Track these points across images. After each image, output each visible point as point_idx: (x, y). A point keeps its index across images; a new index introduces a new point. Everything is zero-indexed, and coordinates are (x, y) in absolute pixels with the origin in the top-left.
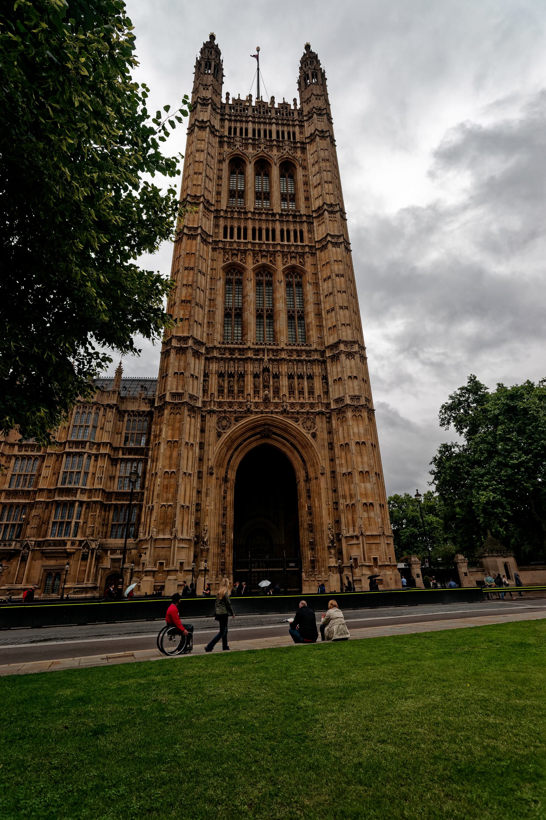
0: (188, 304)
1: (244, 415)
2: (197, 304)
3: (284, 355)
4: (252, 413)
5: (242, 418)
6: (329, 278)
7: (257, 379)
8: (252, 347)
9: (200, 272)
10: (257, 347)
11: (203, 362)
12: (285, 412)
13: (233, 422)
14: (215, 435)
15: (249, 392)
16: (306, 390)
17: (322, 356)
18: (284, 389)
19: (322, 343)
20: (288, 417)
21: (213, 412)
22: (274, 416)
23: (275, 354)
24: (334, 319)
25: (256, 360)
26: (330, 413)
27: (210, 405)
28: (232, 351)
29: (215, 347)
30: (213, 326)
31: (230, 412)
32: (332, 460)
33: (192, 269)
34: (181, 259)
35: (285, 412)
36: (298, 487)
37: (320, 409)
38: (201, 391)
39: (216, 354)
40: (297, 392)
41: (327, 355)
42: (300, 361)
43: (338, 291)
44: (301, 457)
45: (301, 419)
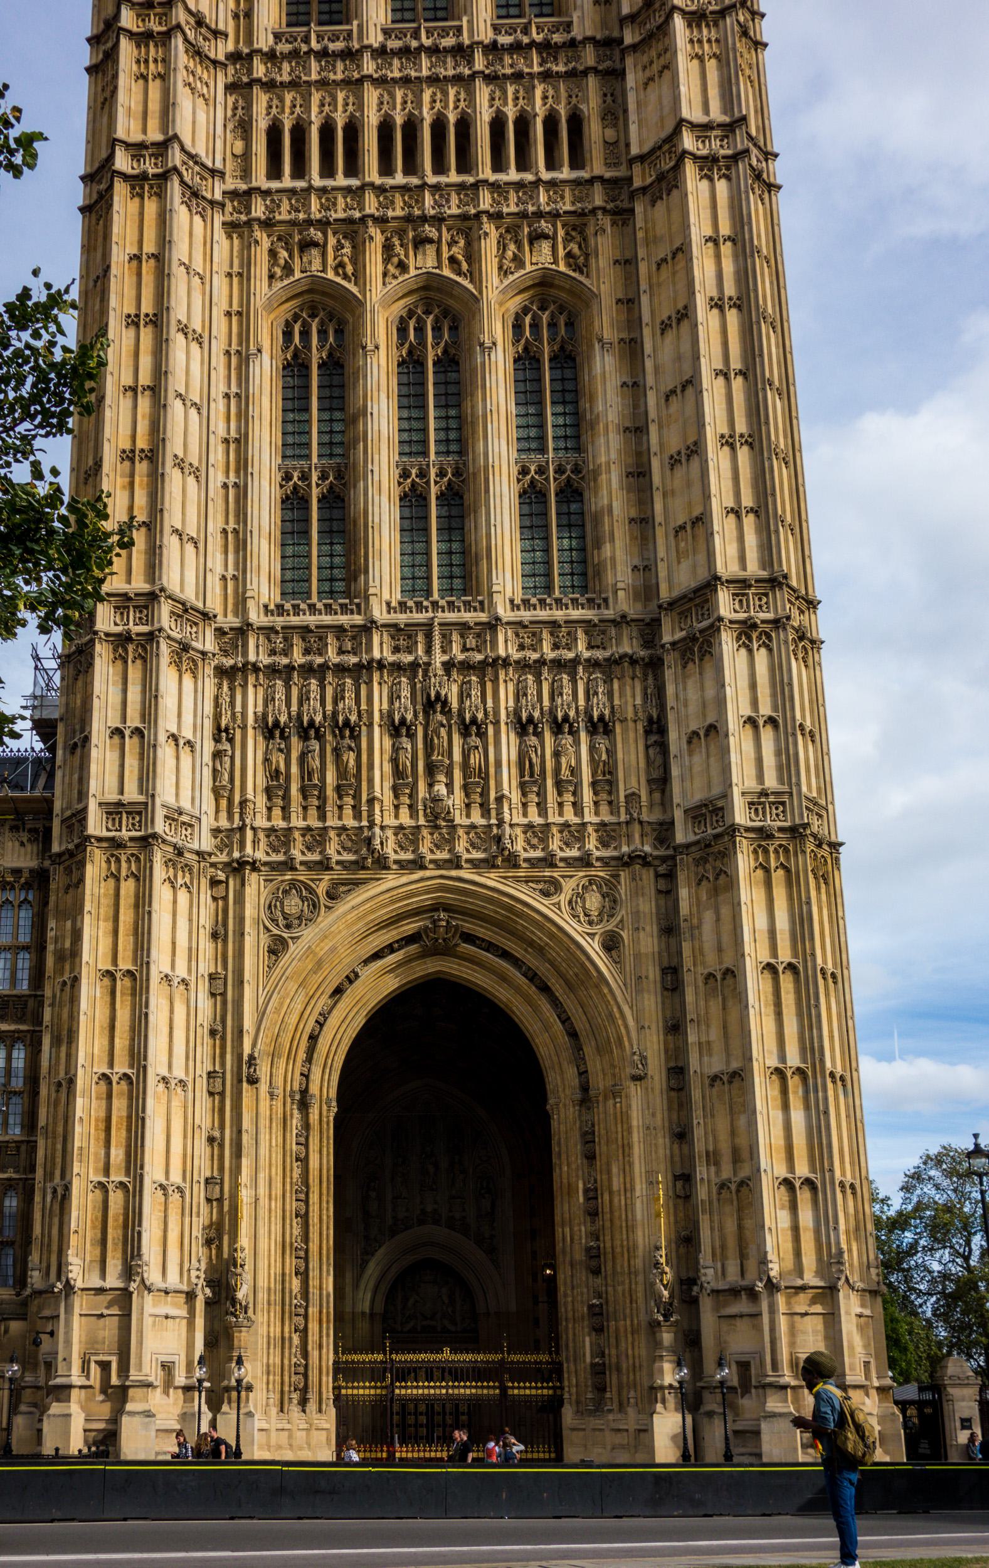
13: (323, 899)
20: (517, 879)
22: (464, 874)
36: (554, 1124)
44: (565, 1020)
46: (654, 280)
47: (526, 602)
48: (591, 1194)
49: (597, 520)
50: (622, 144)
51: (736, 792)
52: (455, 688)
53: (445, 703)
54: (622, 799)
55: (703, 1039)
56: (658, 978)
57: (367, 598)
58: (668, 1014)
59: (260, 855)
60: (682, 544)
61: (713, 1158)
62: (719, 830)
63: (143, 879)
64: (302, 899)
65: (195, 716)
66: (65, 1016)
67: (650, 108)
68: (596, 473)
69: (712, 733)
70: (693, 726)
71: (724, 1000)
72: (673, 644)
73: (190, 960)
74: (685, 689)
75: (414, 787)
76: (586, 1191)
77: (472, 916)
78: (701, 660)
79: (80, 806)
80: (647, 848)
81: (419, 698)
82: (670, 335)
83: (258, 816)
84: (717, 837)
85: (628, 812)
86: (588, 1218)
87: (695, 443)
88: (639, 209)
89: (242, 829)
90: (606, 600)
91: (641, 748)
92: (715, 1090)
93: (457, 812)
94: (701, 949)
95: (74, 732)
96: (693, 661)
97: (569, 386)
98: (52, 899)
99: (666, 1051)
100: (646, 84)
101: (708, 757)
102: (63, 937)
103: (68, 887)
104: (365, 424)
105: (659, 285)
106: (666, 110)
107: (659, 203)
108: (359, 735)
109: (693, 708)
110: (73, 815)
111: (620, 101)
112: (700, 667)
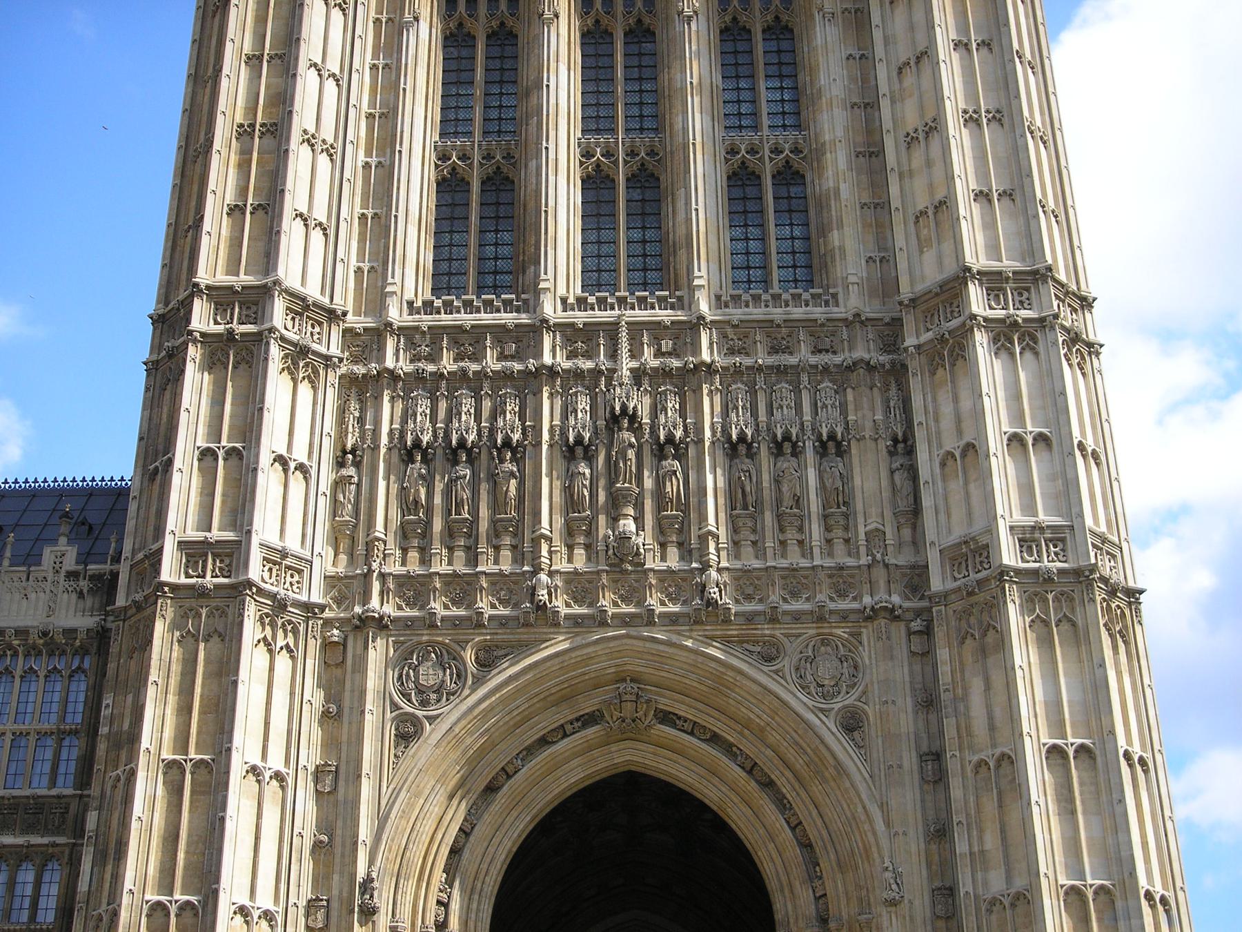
4: (557, 625)
19: (886, 286)
21: (381, 624)
25: (578, 374)
32: (940, 833)
37: (882, 595)
39: (394, 358)
42: (781, 371)
47: (736, 299)
49: (822, 204)
52: (647, 400)
53: (633, 418)
54: (862, 536)
56: (915, 767)
57: (537, 292)
58: (931, 814)
59: (389, 609)
60: (925, 232)
63: (230, 639)
68: (820, 152)
69: (971, 453)
70: (948, 447)
71: (1000, 794)
72: (918, 347)
74: (934, 400)
75: (592, 521)
78: (953, 365)
79: (155, 547)
80: (896, 599)
81: (601, 412)
84: (980, 583)
89: (367, 576)
90: (835, 296)
91: (884, 474)
96: (943, 366)
97: (786, 58)
98: (111, 666)
99: (929, 865)
101: (966, 483)
104: (540, 98)
108: (523, 458)
109: (947, 423)
112: (952, 373)
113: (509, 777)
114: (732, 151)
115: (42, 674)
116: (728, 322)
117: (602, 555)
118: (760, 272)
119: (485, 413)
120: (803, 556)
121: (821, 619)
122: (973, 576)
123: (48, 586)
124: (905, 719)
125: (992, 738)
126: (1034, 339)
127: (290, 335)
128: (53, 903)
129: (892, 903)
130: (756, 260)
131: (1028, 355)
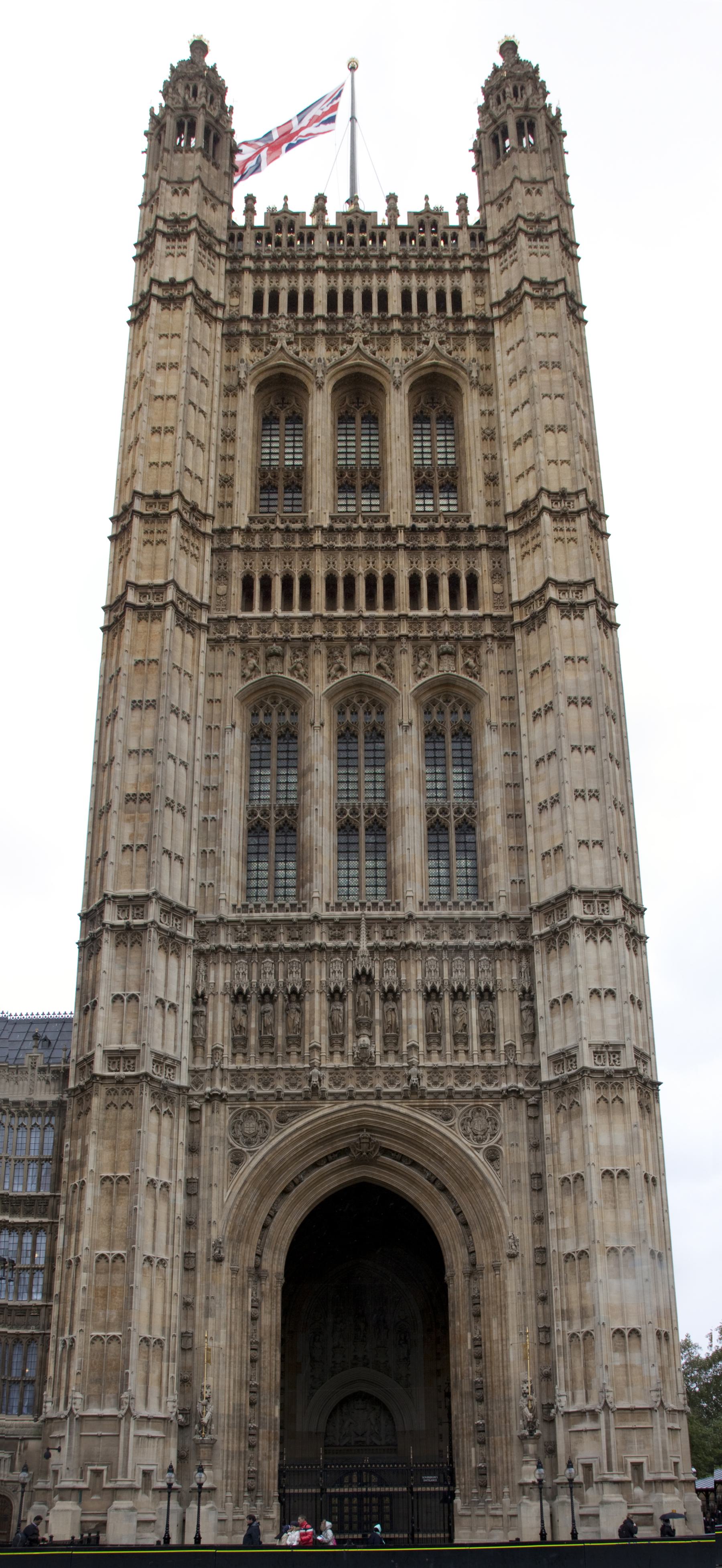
0: (145, 805)
1: (304, 1104)
2: (170, 804)
3: (414, 936)
5: (298, 1112)
6: (549, 708)
7: (338, 1005)
8: (325, 914)
9: (175, 711)
10: (338, 915)
11: (189, 963)
12: (413, 1092)
14: (227, 1161)
15: (316, 1042)
16: (474, 1030)
17: (522, 935)
18: (414, 1030)
19: (523, 899)
20: (423, 1108)
21: (222, 1098)
22: (384, 1104)
23: (389, 932)
24: (557, 830)
25: (337, 950)
26: (539, 1092)
27: (212, 1081)
28: (269, 928)
29: (221, 922)
30: (217, 862)
31: (265, 1097)
32: (540, 1219)
33: (152, 705)
34: (122, 680)
35: (413, 1092)
36: (450, 1291)
38: (187, 1043)
39: (224, 939)
40: (448, 1037)
41: (536, 932)
42: (458, 949)
43: (573, 748)
44: (459, 1213)
45: (459, 1111)
46: (528, 685)
48: (477, 1343)
49: (485, 847)
50: (506, 595)
51: (585, 1044)
52: (377, 966)
54: (502, 1048)
55: (560, 1227)
56: (528, 1182)
59: (225, 1089)
60: (548, 865)
61: (566, 1315)
62: (573, 1071)
64: (259, 1123)
65: (178, 985)
66: (75, 1211)
67: (526, 572)
68: (485, 815)
69: (568, 1001)
70: (555, 996)
71: (575, 1198)
72: (541, 936)
73: (171, 1169)
74: (548, 968)
76: (474, 1340)
77: (388, 1135)
79: (89, 1053)
80: (520, 1085)
81: (350, 973)
82: (540, 722)
83: (225, 1060)
84: (571, 1076)
85: (506, 1058)
86: (474, 1361)
87: (557, 795)
88: (518, 637)
90: (491, 904)
91: (517, 1012)
92: (568, 1264)
93: (378, 1058)
94: (559, 1160)
95: (87, 999)
98: (68, 1123)
99: (533, 1235)
100: (523, 557)
101: (565, 1018)
102: (76, 1151)
103: (80, 1114)
105: (532, 688)
106: (538, 573)
107: (532, 633)
109: (555, 982)
110: (85, 1060)
111: (504, 566)
113: (296, 1185)
114: (431, 812)
115: (29, 1127)
116: (426, 919)
117: (350, 1058)
118: (445, 888)
119: (281, 974)
120: (467, 1059)
121: (477, 1097)
122: (566, 1072)
123: (29, 1076)
124: (523, 1154)
125: (573, 1166)
126: (609, 933)
127: (163, 926)
128: (43, 1254)
129: (512, 1256)
130: (444, 881)
131: (605, 942)
